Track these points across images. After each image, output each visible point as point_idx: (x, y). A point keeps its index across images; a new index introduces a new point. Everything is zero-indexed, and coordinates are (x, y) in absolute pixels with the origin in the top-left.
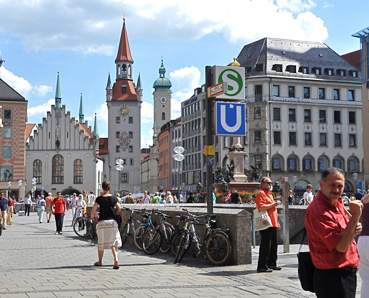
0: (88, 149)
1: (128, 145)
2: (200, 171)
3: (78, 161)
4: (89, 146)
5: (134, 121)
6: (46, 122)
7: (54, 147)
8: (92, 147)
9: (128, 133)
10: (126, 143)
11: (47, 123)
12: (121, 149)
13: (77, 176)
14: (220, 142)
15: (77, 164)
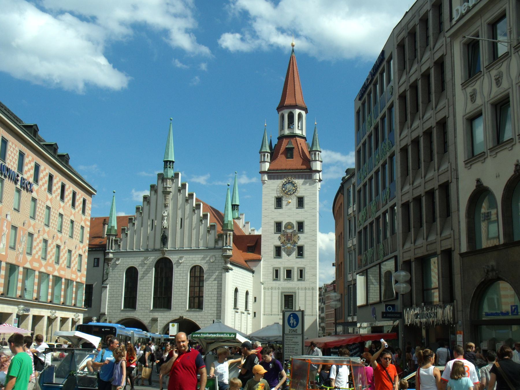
0: (215, 248)
1: (294, 246)
2: (396, 257)
3: (198, 270)
4: (216, 242)
5: (306, 206)
6: (149, 203)
7: (158, 246)
8: (220, 244)
9: (295, 224)
10: (291, 242)
11: (150, 205)
12: (283, 254)
13: (194, 298)
14: (455, 143)
15: (197, 275)
